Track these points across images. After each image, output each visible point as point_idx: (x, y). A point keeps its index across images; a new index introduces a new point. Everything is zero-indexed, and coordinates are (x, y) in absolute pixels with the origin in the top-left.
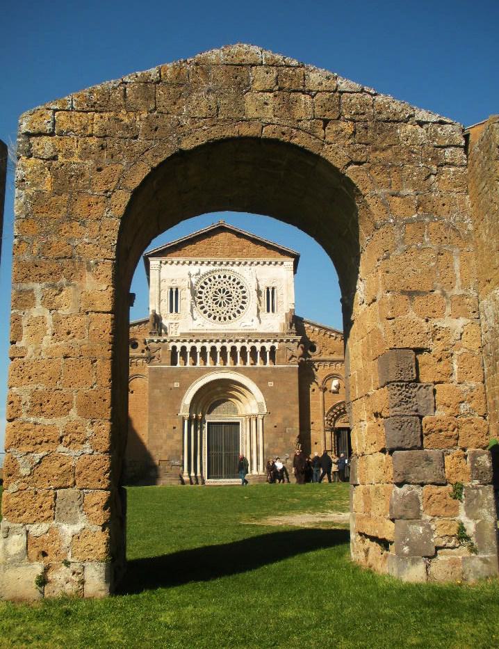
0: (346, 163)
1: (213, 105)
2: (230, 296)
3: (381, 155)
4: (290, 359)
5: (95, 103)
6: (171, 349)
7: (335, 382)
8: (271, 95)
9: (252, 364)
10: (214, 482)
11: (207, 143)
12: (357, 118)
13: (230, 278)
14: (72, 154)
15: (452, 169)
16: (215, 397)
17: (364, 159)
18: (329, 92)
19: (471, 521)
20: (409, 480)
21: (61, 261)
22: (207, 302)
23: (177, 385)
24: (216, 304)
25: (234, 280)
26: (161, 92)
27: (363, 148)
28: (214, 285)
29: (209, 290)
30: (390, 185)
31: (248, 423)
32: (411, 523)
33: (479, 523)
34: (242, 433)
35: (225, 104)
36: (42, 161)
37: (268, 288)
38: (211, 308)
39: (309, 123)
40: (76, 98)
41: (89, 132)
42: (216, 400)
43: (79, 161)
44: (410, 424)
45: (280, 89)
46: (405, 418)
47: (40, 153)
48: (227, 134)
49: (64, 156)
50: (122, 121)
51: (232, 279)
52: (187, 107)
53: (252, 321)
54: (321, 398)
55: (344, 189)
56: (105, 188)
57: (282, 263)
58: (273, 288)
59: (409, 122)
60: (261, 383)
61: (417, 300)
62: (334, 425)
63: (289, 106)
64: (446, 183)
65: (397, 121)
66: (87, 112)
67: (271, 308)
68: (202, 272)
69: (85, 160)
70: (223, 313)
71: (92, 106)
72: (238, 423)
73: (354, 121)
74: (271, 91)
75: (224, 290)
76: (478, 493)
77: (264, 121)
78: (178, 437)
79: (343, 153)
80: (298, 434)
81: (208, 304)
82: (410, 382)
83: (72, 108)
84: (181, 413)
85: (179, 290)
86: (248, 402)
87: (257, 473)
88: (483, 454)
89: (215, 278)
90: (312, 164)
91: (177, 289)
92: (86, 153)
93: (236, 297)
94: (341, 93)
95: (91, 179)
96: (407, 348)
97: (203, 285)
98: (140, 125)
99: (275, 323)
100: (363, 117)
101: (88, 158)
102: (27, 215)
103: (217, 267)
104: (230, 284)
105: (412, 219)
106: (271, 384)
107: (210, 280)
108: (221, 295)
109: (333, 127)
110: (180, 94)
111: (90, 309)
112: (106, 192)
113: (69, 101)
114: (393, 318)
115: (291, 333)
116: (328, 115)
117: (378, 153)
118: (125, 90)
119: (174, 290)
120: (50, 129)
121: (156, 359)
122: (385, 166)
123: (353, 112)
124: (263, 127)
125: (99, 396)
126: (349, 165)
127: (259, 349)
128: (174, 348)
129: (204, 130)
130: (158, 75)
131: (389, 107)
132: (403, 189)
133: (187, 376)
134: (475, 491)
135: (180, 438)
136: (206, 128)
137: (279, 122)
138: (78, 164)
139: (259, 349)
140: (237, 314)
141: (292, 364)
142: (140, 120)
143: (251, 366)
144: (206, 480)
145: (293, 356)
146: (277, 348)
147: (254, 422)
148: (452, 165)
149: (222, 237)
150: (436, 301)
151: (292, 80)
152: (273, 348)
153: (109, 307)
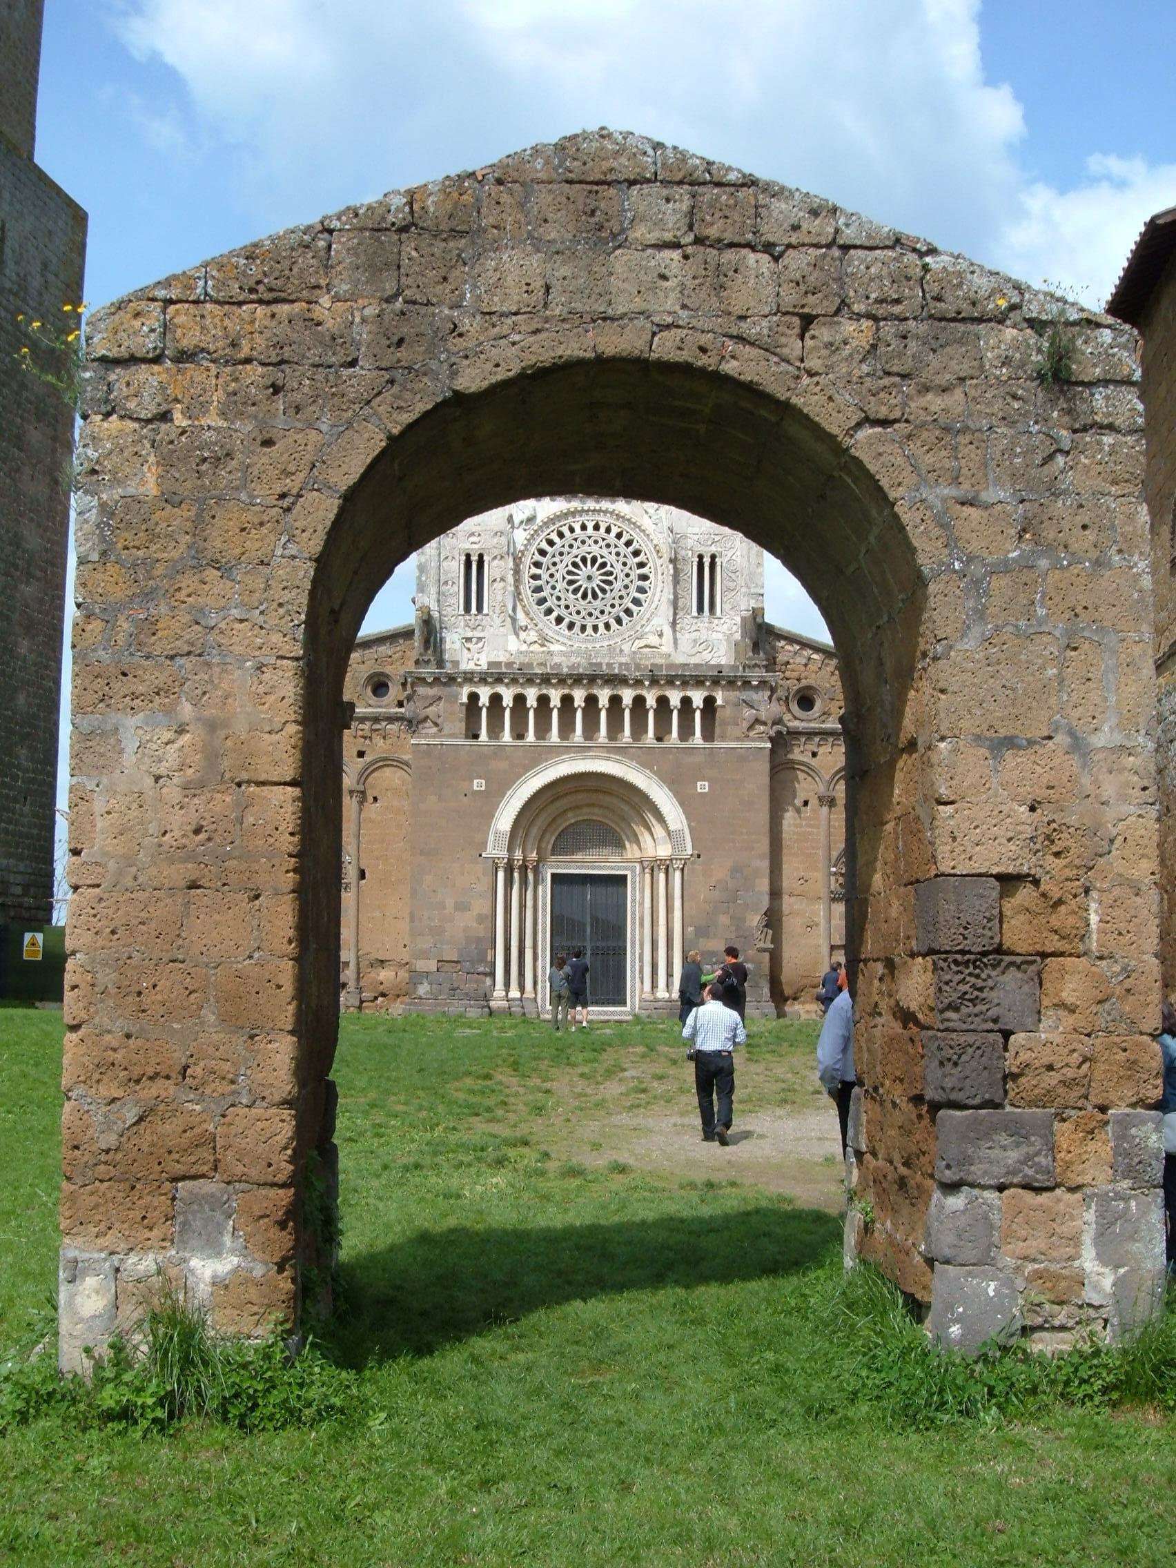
0: (853, 424)
1: (538, 284)
3: (936, 402)
4: (751, 728)
5: (258, 283)
6: (465, 700)
8: (676, 255)
11: (522, 376)
12: (881, 311)
13: (608, 530)
14: (204, 407)
15: (1108, 440)
16: (570, 814)
17: (896, 414)
18: (817, 246)
19: (1106, 1270)
20: (970, 1179)
21: (180, 661)
23: (479, 785)
24: (576, 591)
25: (619, 536)
26: (414, 253)
27: (894, 385)
28: (571, 546)
29: (557, 559)
30: (958, 478)
31: (648, 876)
32: (969, 1274)
33: (1124, 1275)
34: (633, 901)
35: (564, 278)
36: (136, 425)
37: (701, 557)
38: (563, 603)
39: (765, 323)
40: (214, 273)
41: (245, 352)
43: (222, 423)
44: (980, 1052)
45: (699, 241)
46: (970, 1037)
47: (132, 405)
48: (569, 352)
49: (188, 413)
50: (319, 324)
51: (613, 534)
52: (475, 287)
53: (661, 635)
54: (824, 823)
55: (849, 481)
56: (278, 488)
58: (713, 557)
59: (1008, 322)
60: (677, 783)
61: (1011, 758)
63: (719, 280)
64: (1092, 473)
65: (980, 320)
66: (240, 304)
67: (706, 604)
68: (541, 517)
69: (233, 423)
70: (590, 614)
71: (252, 291)
72: (622, 880)
73: (875, 319)
74: (676, 245)
76: (1127, 1208)
77: (656, 319)
79: (845, 397)
80: (765, 903)
81: (556, 593)
82: (985, 954)
83: (206, 294)
87: (667, 995)
88: (1144, 1122)
89: (572, 530)
90: (773, 419)
91: (481, 556)
92: (235, 405)
93: (622, 576)
94: (846, 248)
95: (248, 466)
96: (980, 875)
97: (544, 546)
98: (364, 334)
100: (897, 309)
101: (240, 415)
102: (104, 553)
104: (608, 546)
105: (1006, 560)
106: (702, 787)
107: (561, 535)
108: (585, 571)
109: (822, 332)
110: (459, 255)
111: (244, 776)
112: (283, 496)
113: (199, 278)
114: (952, 803)
115: (756, 665)
116: (814, 305)
117: (930, 396)
118: (329, 247)
120: (155, 348)
121: (429, 723)
122: (946, 429)
123: (873, 296)
124: (654, 334)
125: (267, 977)
126: (859, 425)
128: (474, 697)
129: (514, 344)
130: (407, 209)
131: (960, 285)
132: (987, 488)
133: (504, 765)
134: (1122, 1205)
135: (486, 910)
136: (517, 338)
137: (694, 323)
138: (217, 430)
141: (753, 740)
142: (363, 321)
145: (757, 721)
146: (719, 702)
147: (662, 876)
148: (1111, 428)
150: (1056, 762)
151: (726, 217)
152: (709, 701)
153: (288, 770)
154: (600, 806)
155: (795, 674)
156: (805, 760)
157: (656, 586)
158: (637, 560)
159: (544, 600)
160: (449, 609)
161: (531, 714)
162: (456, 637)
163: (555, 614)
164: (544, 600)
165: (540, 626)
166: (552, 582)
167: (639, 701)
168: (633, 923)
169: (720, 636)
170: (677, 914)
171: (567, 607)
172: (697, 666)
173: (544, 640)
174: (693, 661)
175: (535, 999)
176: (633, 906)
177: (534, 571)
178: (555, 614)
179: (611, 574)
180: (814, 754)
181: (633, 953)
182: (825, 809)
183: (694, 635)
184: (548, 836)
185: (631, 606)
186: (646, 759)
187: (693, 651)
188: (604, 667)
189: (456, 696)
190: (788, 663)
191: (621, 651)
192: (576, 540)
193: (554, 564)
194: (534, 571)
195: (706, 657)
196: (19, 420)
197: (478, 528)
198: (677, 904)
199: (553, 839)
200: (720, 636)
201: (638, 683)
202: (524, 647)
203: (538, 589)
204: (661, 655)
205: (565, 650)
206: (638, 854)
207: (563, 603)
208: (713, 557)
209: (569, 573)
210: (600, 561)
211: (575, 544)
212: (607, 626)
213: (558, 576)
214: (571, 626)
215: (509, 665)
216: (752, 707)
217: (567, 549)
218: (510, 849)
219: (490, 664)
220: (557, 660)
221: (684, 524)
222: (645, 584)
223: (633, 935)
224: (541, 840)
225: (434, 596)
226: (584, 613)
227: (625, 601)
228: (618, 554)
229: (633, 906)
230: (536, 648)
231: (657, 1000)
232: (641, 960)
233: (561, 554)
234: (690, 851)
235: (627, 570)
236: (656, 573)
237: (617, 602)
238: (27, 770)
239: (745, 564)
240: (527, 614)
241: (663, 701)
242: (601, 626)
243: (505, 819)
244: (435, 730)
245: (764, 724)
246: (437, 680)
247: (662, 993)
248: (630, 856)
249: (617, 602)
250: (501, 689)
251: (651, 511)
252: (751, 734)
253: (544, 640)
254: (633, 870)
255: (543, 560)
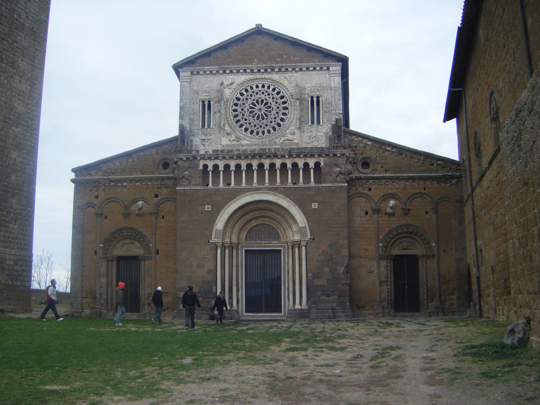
2: (270, 107)
6: (201, 168)
7: (392, 203)
9: (294, 184)
10: (253, 316)
13: (269, 87)
16: (253, 221)
22: (243, 115)
23: (208, 208)
25: (274, 90)
28: (251, 95)
29: (245, 102)
31: (290, 250)
34: (284, 262)
37: (312, 98)
42: (255, 224)
51: (271, 89)
57: (328, 69)
58: (318, 97)
62: (390, 253)
67: (316, 120)
75: (262, 101)
78: (209, 266)
81: (245, 117)
84: (214, 240)
85: (212, 103)
86: (290, 227)
87: (300, 307)
89: (252, 88)
91: (209, 102)
93: (275, 108)
97: (239, 96)
99: (319, 136)
103: (251, 76)
104: (269, 95)
106: (315, 206)
107: (247, 91)
119: (206, 103)
121: (184, 180)
127: (301, 165)
135: (212, 268)
139: (301, 165)
140: (277, 128)
141: (339, 182)
143: (292, 186)
144: (244, 314)
146: (322, 164)
147: (297, 249)
149: (260, 42)
152: (317, 165)
154: (268, 217)
155: (360, 152)
156: (365, 192)
157: (291, 111)
158: (283, 100)
159: (239, 121)
160: (194, 127)
161: (233, 173)
162: (198, 139)
163: (244, 127)
164: (239, 121)
165: (237, 132)
166: (243, 112)
167: (284, 165)
168: (284, 273)
169: (322, 134)
170: (304, 267)
171: (250, 124)
172: (311, 148)
173: (238, 139)
174: (309, 146)
175: (237, 311)
176: (284, 265)
177: (234, 107)
178: (244, 127)
179: (270, 107)
180: (370, 190)
181: (284, 287)
182: (376, 216)
183: (309, 134)
184: (243, 231)
185: (279, 121)
186: (287, 193)
187: (309, 142)
188: (267, 150)
189: (197, 166)
190: (356, 147)
191: (275, 142)
192: (253, 92)
193: (244, 104)
194: (234, 107)
195: (316, 144)
196: (12, 56)
197: (208, 89)
198: (304, 262)
199: (246, 233)
200: (322, 134)
201: (283, 156)
202: (229, 143)
203: (236, 116)
204: (294, 144)
205: (248, 142)
206: (285, 240)
207: (248, 121)
208: (318, 97)
209: (251, 108)
210: (265, 101)
211: (253, 95)
212: (269, 132)
213: (246, 109)
214: (252, 132)
215: (222, 151)
216: (338, 167)
217: (249, 97)
218: (223, 238)
219: (214, 151)
220: (245, 148)
221: (304, 83)
222: (286, 111)
223: (284, 279)
224: (239, 234)
225: (188, 121)
226: (257, 126)
227: (277, 120)
228: (273, 98)
229: (284, 265)
230: (235, 143)
231: (295, 310)
232: (288, 290)
233: (247, 99)
234: (309, 237)
235: (278, 105)
236: (291, 106)
237: (273, 120)
238: (16, 209)
239: (333, 100)
240: (231, 127)
241: (295, 165)
242: (266, 131)
243: (220, 224)
244: (187, 183)
245: (344, 174)
246: (188, 159)
247: (297, 306)
248: (282, 241)
249: (273, 120)
250: (217, 162)
251: (288, 78)
252: (338, 179)
253: (238, 139)
254: (284, 247)
255: (239, 102)
